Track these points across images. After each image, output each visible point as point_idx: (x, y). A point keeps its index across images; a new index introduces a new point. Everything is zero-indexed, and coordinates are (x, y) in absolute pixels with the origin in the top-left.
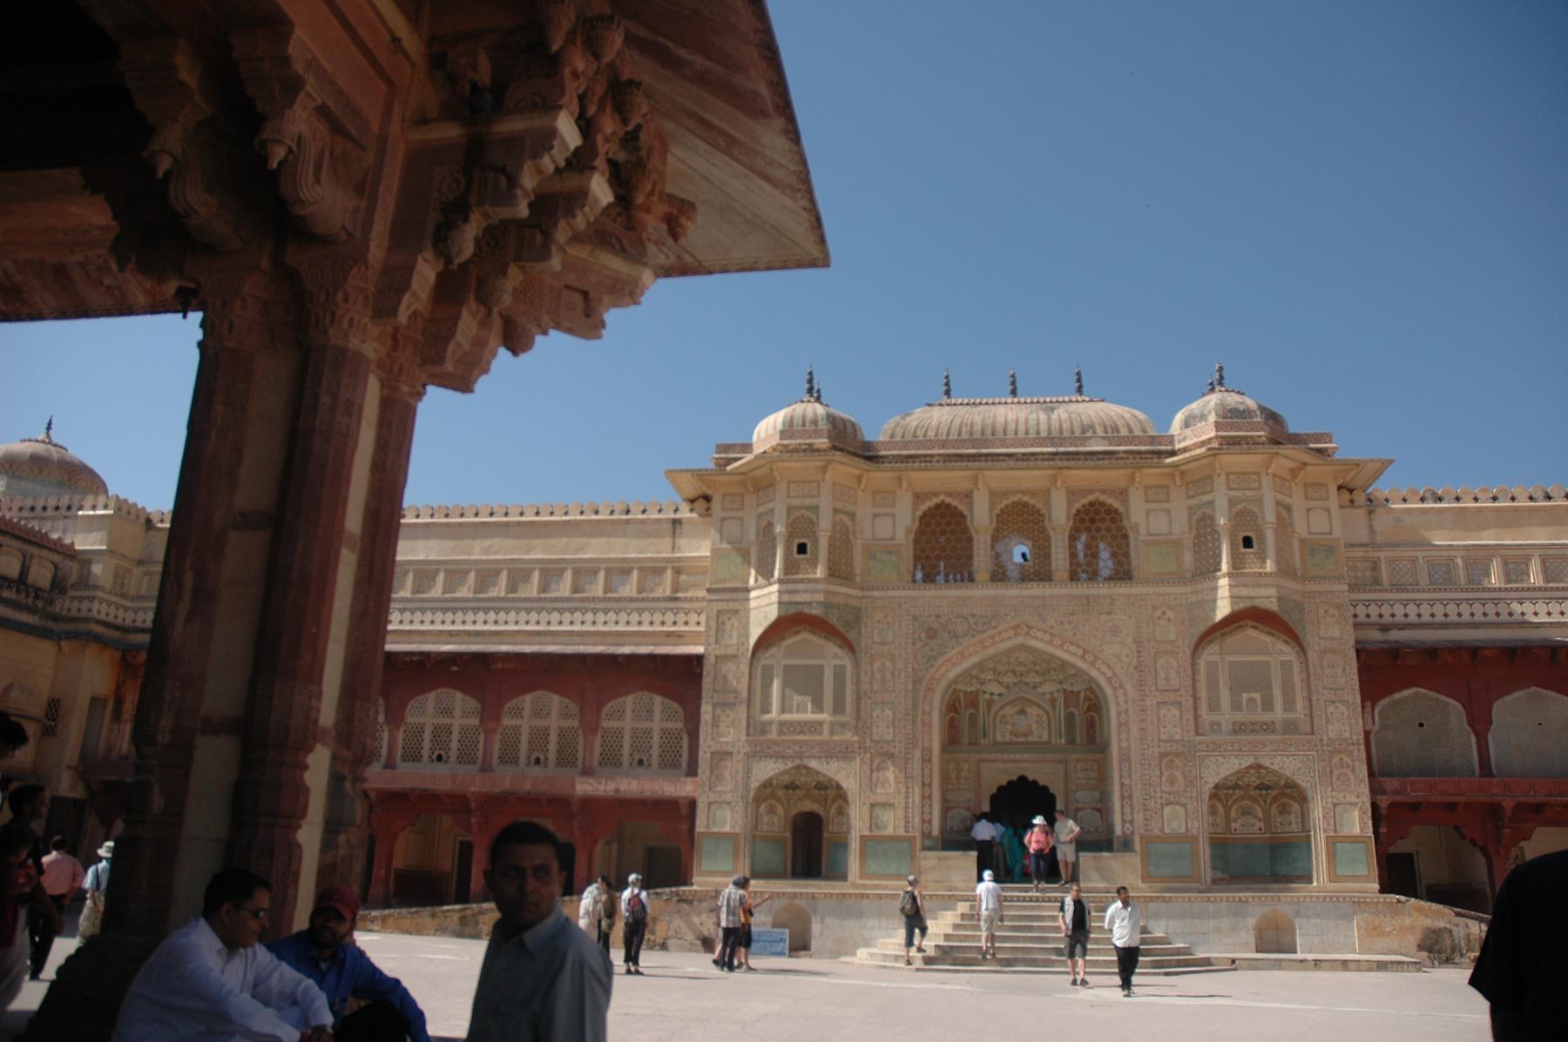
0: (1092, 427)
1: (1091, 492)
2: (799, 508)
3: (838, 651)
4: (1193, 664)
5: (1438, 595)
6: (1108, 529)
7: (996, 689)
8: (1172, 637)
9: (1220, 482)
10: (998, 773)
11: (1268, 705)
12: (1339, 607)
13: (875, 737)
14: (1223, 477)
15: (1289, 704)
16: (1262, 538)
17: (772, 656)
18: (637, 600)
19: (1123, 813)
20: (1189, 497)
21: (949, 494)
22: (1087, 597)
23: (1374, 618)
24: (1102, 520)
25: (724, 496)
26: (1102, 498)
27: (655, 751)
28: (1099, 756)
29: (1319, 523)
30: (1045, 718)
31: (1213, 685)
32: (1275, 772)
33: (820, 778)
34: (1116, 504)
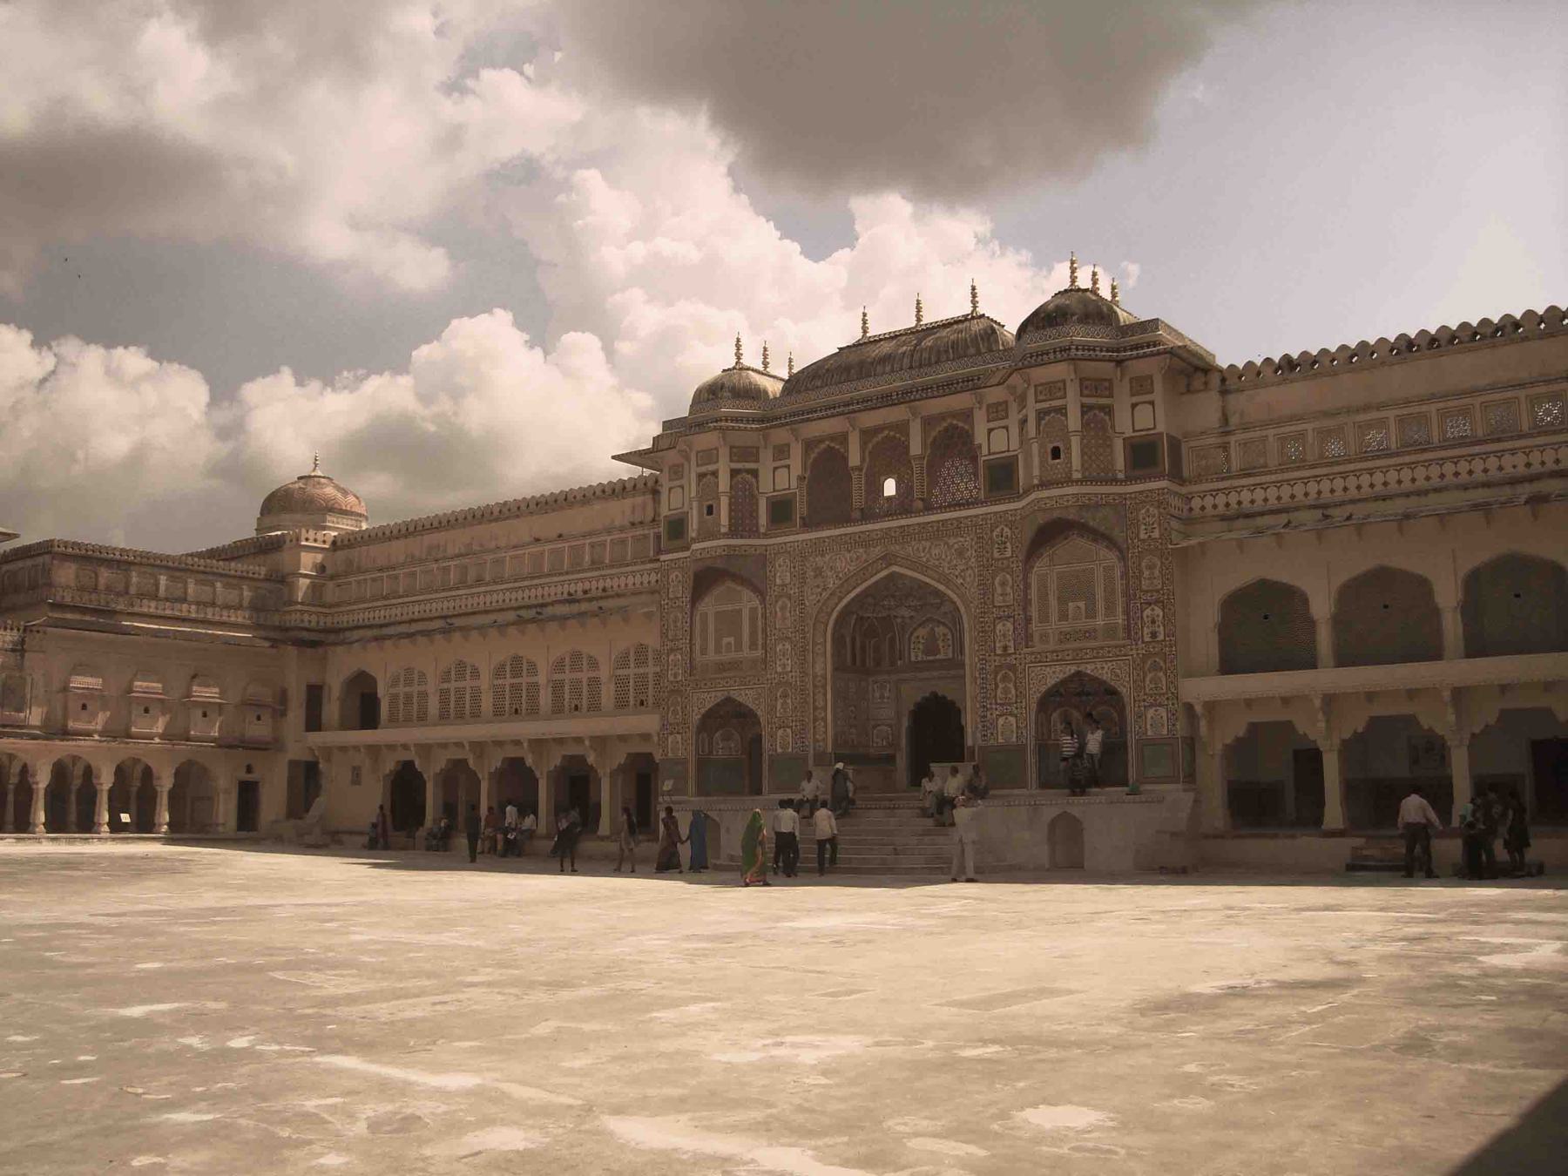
0: (947, 352)
1: (942, 417)
4: (1025, 578)
5: (1286, 476)
7: (906, 613)
11: (1091, 613)
13: (779, 669)
15: (1110, 609)
16: (1069, 448)
21: (832, 438)
23: (1221, 509)
29: (1144, 418)
31: (1043, 597)
32: (1094, 679)
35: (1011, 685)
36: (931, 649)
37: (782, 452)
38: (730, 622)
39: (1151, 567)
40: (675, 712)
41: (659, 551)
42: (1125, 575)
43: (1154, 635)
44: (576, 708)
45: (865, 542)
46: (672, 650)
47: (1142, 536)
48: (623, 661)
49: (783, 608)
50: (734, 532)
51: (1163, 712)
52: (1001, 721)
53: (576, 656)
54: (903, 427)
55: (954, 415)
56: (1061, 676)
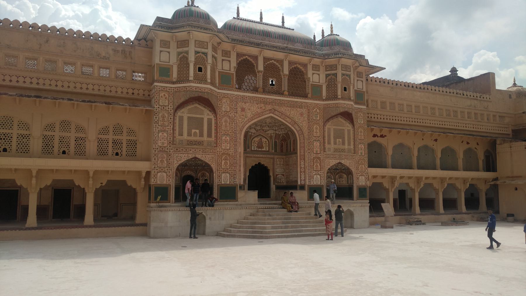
1: (296, 64)
2: (198, 52)
3: (210, 113)
8: (318, 119)
9: (339, 67)
10: (252, 162)
11: (343, 144)
13: (223, 147)
15: (349, 144)
16: (349, 89)
17: (183, 112)
19: (301, 177)
20: (326, 71)
21: (249, 56)
22: (294, 101)
25: (161, 41)
26: (299, 66)
27: (124, 149)
30: (267, 142)
33: (199, 162)
34: (303, 70)
35: (318, 164)
39: (361, 132)
40: (162, 161)
42: (354, 133)
43: (361, 153)
44: (64, 152)
45: (265, 102)
48: (105, 131)
49: (226, 121)
50: (212, 83)
51: (363, 178)
52: (315, 176)
53: (65, 125)
54: (281, 62)
55: (300, 64)
56: (334, 163)
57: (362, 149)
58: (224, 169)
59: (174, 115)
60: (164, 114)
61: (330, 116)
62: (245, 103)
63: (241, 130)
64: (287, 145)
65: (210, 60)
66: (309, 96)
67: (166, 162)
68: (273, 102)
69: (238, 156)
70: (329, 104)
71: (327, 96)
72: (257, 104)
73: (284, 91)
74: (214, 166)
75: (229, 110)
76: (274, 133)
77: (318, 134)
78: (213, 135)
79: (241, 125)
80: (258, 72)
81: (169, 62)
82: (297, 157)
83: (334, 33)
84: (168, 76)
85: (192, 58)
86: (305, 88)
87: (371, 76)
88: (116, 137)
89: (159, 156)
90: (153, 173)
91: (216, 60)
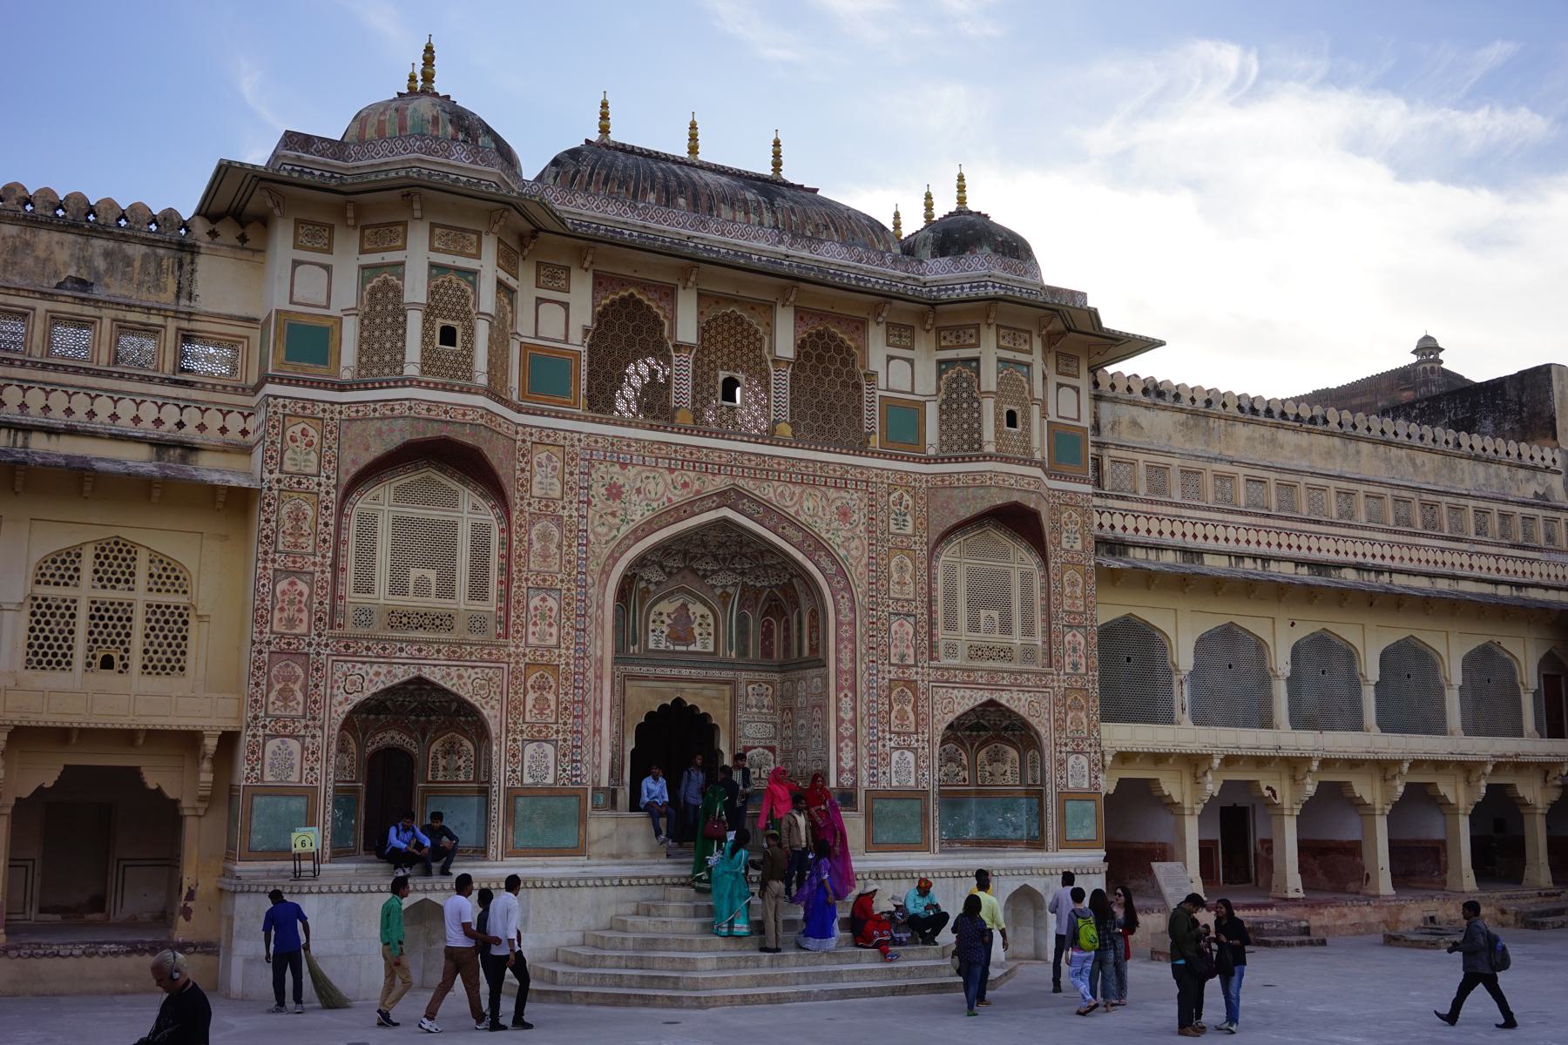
1: (822, 316)
3: (480, 502)
4: (929, 567)
6: (838, 373)
9: (989, 338)
10: (648, 698)
11: (1006, 628)
12: (1085, 512)
13: (531, 640)
14: (993, 328)
15: (1028, 630)
18: (109, 375)
19: (839, 759)
21: (645, 286)
24: (832, 360)
28: (776, 677)
30: (711, 620)
31: (951, 596)
35: (909, 708)
36: (682, 633)
37: (553, 275)
38: (439, 543)
39: (1073, 584)
40: (286, 695)
41: (265, 379)
43: (1075, 666)
45: (700, 463)
46: (288, 573)
47: (1065, 545)
49: (545, 537)
50: (492, 393)
51: (1083, 760)
52: (896, 755)
56: (971, 704)
57: (1079, 647)
58: (532, 725)
59: (340, 513)
60: (298, 509)
61: (954, 521)
62: (624, 466)
63: (605, 572)
64: (787, 629)
65: (487, 299)
66: (875, 442)
67: (300, 697)
68: (732, 463)
69: (590, 674)
70: (950, 474)
71: (942, 443)
72: (671, 471)
73: (776, 422)
74: (492, 714)
75: (557, 494)
76: (735, 585)
77: (910, 589)
78: (494, 588)
79: (607, 551)
80: (678, 347)
81: (327, 307)
82: (825, 678)
83: (972, 205)
84: (324, 361)
85: (416, 288)
86: (858, 411)
87: (1111, 369)
88: (109, 595)
89: (274, 671)
90: (245, 739)
91: (511, 302)
